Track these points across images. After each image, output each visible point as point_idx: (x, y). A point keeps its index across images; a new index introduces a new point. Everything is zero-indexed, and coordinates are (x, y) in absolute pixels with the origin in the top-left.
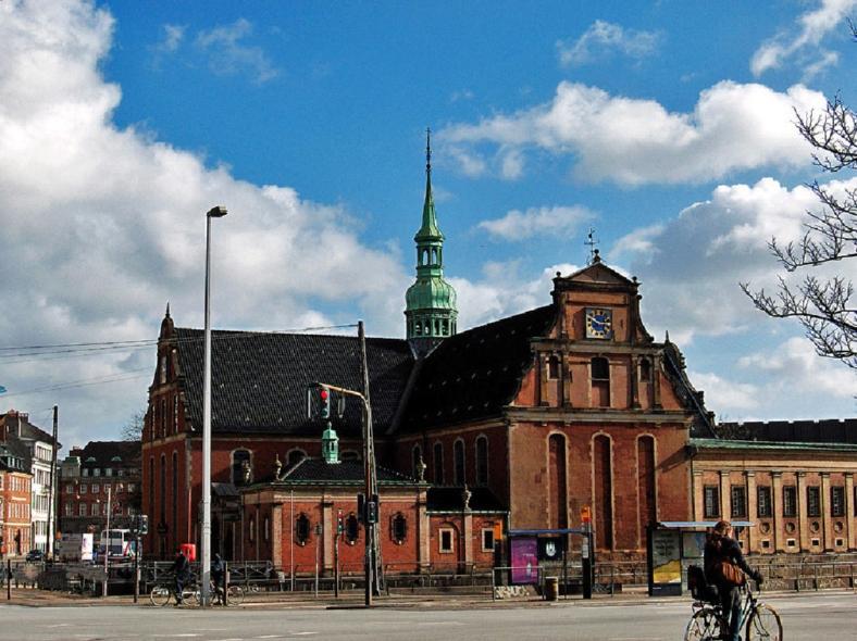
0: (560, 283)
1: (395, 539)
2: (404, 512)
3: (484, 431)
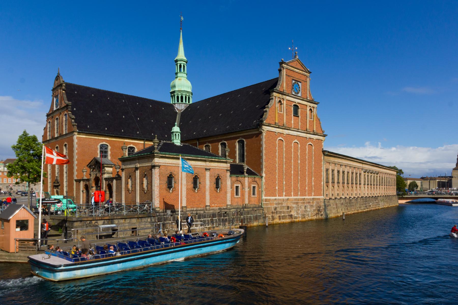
1: (216, 189)
2: (220, 174)
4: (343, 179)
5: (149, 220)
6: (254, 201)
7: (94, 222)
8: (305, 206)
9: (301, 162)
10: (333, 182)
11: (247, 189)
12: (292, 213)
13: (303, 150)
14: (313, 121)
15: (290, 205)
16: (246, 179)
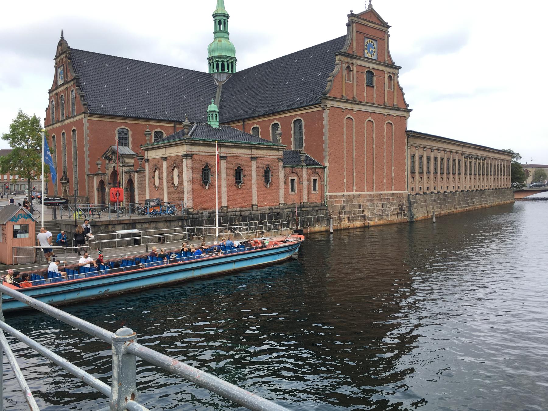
0: (353, 18)
2: (270, 164)
3: (300, 115)
4: (435, 169)
5: (180, 224)
6: (315, 198)
7: (110, 227)
8: (383, 204)
9: (376, 146)
10: (421, 173)
11: (305, 183)
12: (366, 213)
14: (394, 92)
15: (362, 204)
16: (305, 170)
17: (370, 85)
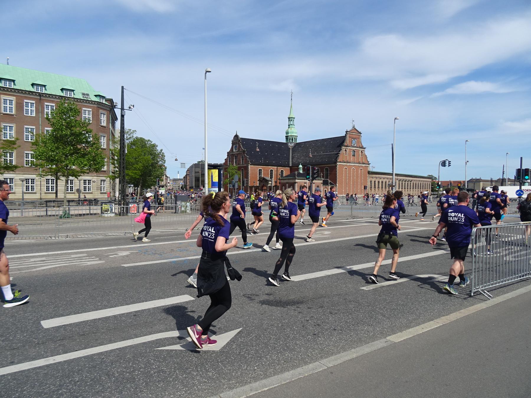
10: (375, 187)
13: (357, 172)
17: (354, 156)
